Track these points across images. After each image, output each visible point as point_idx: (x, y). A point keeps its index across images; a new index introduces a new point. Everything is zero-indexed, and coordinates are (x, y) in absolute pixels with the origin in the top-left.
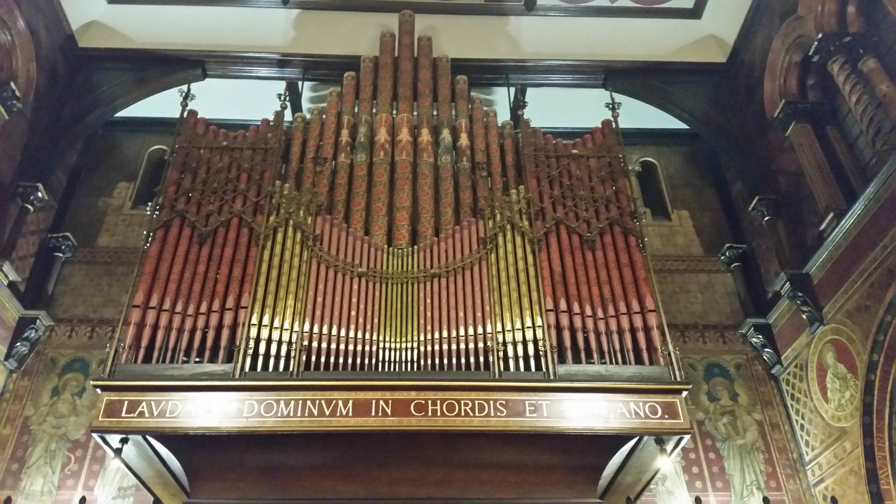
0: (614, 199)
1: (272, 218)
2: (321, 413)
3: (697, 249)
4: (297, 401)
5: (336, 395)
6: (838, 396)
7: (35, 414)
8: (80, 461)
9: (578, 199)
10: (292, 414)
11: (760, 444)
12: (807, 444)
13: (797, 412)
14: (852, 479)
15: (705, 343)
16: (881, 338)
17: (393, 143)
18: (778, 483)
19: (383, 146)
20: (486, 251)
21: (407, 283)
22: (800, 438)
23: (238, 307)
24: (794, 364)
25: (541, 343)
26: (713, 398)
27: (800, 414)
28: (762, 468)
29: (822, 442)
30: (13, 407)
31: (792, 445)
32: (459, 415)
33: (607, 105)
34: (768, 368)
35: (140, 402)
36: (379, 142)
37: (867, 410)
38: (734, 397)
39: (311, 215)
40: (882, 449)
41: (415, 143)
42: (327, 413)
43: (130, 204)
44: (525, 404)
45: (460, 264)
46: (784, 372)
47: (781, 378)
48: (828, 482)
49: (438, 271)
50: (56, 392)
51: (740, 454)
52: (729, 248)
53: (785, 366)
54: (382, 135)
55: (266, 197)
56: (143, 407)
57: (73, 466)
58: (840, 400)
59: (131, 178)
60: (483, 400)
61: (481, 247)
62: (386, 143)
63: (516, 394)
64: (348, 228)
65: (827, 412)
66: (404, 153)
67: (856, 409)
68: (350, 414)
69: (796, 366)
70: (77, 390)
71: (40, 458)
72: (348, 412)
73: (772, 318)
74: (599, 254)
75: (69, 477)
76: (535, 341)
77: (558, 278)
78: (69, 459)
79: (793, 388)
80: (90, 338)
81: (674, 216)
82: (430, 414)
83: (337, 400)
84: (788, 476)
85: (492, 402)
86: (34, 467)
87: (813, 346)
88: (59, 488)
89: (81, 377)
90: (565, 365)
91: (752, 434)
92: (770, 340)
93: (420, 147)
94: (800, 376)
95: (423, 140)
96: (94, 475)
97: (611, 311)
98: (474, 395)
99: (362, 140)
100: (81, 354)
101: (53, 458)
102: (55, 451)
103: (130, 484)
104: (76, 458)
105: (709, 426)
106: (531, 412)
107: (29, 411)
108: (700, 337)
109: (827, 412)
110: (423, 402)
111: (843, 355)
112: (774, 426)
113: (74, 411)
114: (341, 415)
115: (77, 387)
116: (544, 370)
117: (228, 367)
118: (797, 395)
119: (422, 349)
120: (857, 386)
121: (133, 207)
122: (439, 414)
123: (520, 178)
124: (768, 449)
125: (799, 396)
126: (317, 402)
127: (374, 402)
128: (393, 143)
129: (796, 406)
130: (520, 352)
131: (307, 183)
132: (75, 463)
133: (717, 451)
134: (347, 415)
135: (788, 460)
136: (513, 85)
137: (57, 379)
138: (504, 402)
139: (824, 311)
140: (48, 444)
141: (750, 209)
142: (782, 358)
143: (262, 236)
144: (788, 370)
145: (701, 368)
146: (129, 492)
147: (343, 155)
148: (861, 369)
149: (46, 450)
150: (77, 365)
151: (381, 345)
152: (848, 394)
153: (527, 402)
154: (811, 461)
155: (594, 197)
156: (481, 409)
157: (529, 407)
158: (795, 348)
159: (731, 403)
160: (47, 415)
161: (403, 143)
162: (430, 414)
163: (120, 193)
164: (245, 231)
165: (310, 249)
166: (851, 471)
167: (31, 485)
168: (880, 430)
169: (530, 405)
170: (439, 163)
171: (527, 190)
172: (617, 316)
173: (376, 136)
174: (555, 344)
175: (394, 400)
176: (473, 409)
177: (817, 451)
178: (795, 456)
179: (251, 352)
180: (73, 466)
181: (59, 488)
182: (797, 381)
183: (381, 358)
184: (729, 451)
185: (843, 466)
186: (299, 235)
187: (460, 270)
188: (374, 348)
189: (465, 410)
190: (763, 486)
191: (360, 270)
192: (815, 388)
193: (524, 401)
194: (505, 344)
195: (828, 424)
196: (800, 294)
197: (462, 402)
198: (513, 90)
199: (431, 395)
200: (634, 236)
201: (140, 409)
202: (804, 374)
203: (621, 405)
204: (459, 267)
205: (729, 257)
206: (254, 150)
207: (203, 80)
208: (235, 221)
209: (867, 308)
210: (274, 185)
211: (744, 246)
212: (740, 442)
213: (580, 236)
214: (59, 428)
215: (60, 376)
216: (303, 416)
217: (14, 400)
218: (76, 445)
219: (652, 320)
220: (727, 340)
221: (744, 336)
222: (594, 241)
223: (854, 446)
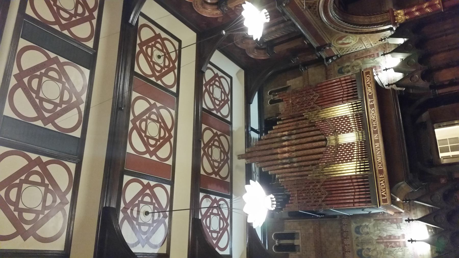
3: (301, 78)
6: (350, 40)
8: (391, 243)
9: (307, 99)
11: (362, 59)
12: (361, 48)
14: (372, 37)
15: (331, 74)
16: (340, 30)
17: (288, 152)
18: (372, 54)
19: (290, 154)
22: (359, 50)
24: (339, 51)
28: (368, 58)
29: (361, 44)
31: (361, 51)
32: (376, 119)
37: (356, 33)
38: (348, 66)
40: (366, 30)
41: (288, 146)
44: (371, 104)
46: (340, 54)
47: (341, 55)
48: (371, 42)
51: (365, 64)
52: (301, 69)
53: (338, 54)
54: (286, 155)
57: (393, 244)
58: (352, 40)
65: (354, 43)
66: (292, 148)
69: (339, 51)
70: (368, 251)
71: (391, 255)
75: (396, 245)
76: (352, 104)
78: (390, 247)
80: (349, 252)
81: (289, 85)
82: (376, 125)
84: (370, 52)
85: (371, 112)
87: (336, 46)
88: (400, 246)
89: (363, 251)
91: (359, 61)
92: (331, 57)
96: (395, 237)
100: (355, 253)
101: (391, 251)
102: (389, 251)
103: (396, 225)
104: (390, 244)
106: (372, 103)
112: (356, 56)
115: (367, 251)
116: (360, 101)
118: (347, 50)
119: (358, 131)
122: (376, 123)
125: (348, 50)
128: (288, 152)
129: (350, 51)
132: (391, 244)
135: (365, 52)
138: (371, 109)
139: (327, 43)
142: (336, 54)
146: (398, 225)
148: (347, 34)
150: (360, 253)
151: (358, 141)
152: (351, 38)
153: (370, 104)
162: (376, 125)
164: (326, 183)
166: (370, 37)
167: (400, 255)
168: (361, 30)
169: (371, 103)
173: (286, 157)
176: (374, 116)
177: (363, 45)
178: (364, 51)
180: (393, 244)
181: (400, 246)
182: (343, 50)
183: (362, 140)
184: (364, 67)
185: (368, 39)
186: (326, 168)
189: (374, 117)
190: (373, 58)
192: (347, 46)
197: (372, 118)
199: (371, 126)
205: (304, 69)
212: (361, 64)
214: (381, 252)
223: (363, 37)
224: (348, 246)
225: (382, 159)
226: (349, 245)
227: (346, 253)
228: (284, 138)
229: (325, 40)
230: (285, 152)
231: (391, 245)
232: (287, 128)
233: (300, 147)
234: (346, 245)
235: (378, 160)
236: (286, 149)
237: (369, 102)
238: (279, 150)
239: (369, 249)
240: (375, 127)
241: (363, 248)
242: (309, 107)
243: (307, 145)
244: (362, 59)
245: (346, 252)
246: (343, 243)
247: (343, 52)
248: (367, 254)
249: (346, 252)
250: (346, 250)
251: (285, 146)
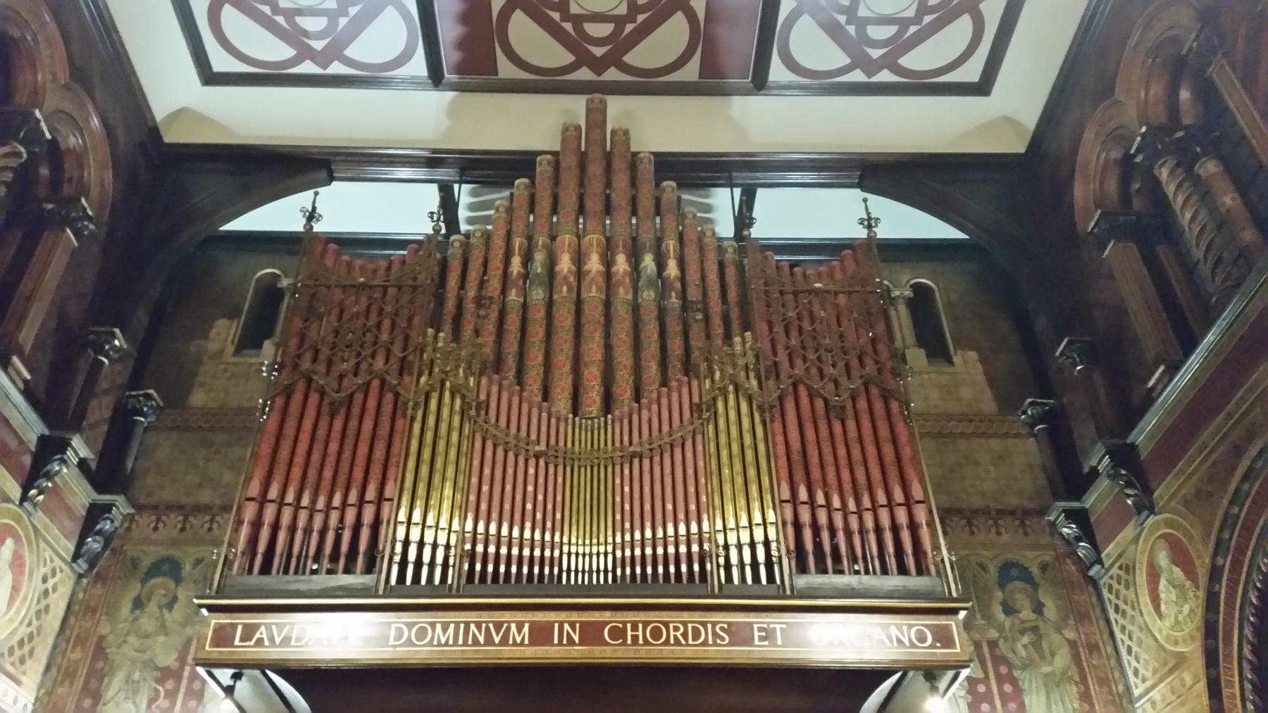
0: (870, 349)
1: (423, 379)
2: (489, 641)
3: (988, 405)
4: (457, 624)
5: (505, 616)
6: (1174, 609)
7: (111, 632)
8: (171, 696)
9: (822, 351)
10: (451, 642)
12: (1136, 673)
13: (1123, 629)
15: (999, 534)
16: (1226, 536)
17: (580, 273)
19: (565, 278)
20: (701, 421)
21: (599, 465)
22: (1127, 665)
23: (380, 498)
24: (1118, 564)
25: (774, 546)
26: (1009, 610)
27: (1127, 632)
29: (1155, 672)
30: (83, 623)
31: (1117, 674)
32: (667, 642)
33: (861, 222)
34: (1084, 567)
35: (257, 626)
36: (561, 274)
37: (1210, 630)
38: (1038, 609)
39: (474, 374)
40: (1230, 684)
41: (608, 274)
42: (497, 640)
43: (231, 349)
44: (752, 629)
45: (667, 440)
46: (1105, 574)
47: (1102, 582)
49: (638, 449)
50: (138, 604)
51: (1046, 686)
52: (1031, 404)
54: (565, 264)
55: (414, 351)
56: (261, 633)
58: (1176, 617)
59: (233, 314)
60: (701, 623)
61: (695, 415)
62: (569, 275)
63: (741, 614)
64: (522, 390)
65: (1160, 631)
67: (1198, 629)
68: (526, 642)
70: (166, 600)
71: (119, 691)
72: (523, 639)
73: (1090, 500)
74: (851, 425)
76: (767, 543)
77: (796, 457)
78: (157, 691)
79: (1118, 598)
80: (183, 529)
81: (957, 359)
82: (629, 642)
83: (509, 622)
85: (709, 626)
86: (111, 705)
87: (1141, 541)
90: (806, 576)
91: (1062, 660)
92: (1087, 531)
93: (614, 279)
94: (1126, 581)
95: (618, 270)
97: (866, 502)
98: (685, 616)
99: (539, 270)
100: (172, 552)
101: (136, 692)
102: (138, 682)
104: (166, 691)
105: (1003, 648)
106: (762, 639)
107: (104, 629)
108: (992, 526)
109: (1160, 631)
110: (621, 626)
111: (1181, 558)
112: (1093, 648)
113: (163, 629)
114: (515, 644)
115: (165, 596)
116: (778, 582)
117: (368, 580)
118: (1122, 606)
119: (619, 554)
120: (1197, 597)
121: (238, 351)
122: (641, 641)
123: (746, 326)
124: (1084, 681)
125: (1125, 607)
126: (484, 625)
127: (556, 625)
128: (580, 273)
129: (1121, 621)
130: (747, 559)
131: (467, 332)
132: (165, 697)
133: (1014, 682)
134: (522, 643)
135: (1111, 693)
136: (738, 185)
137: (139, 585)
138: (726, 626)
139: (1156, 494)
140: (131, 672)
141: (1057, 354)
142: (1103, 555)
143: (411, 404)
144: (1111, 572)
145: (993, 569)
147: (514, 292)
149: (128, 680)
150: (166, 567)
151: (566, 549)
152: (1186, 609)
153: (756, 626)
154: (1141, 697)
155: (843, 347)
156: (696, 635)
157: (759, 631)
158: (1118, 543)
159: (1033, 616)
160: (128, 634)
161: (592, 275)
162: (629, 642)
163: (219, 334)
164: (389, 397)
165: (472, 421)
168: (1228, 657)
169: (760, 630)
170: (640, 301)
171: (755, 339)
172: (874, 510)
174: (792, 547)
175: (583, 624)
176: (685, 635)
177: (1149, 683)
178: (1121, 688)
179: (397, 558)
182: (1121, 587)
183: (565, 567)
184: (1031, 681)
185: (1182, 704)
186: (458, 402)
187: (668, 447)
188: (557, 553)
189: (675, 637)
191: (537, 448)
192: (1145, 599)
193: (751, 624)
194: (726, 547)
195: (1164, 649)
196: (1123, 472)
197: (671, 626)
198: (737, 192)
199: (630, 616)
200: (896, 399)
201: (258, 635)
202: (1130, 578)
203: (879, 629)
204: (666, 443)
205: (1032, 417)
206: (399, 288)
207: (329, 184)
208: (376, 384)
209: (1210, 494)
210: (425, 334)
211: (1052, 401)
212: (1046, 669)
213: (826, 401)
215: (144, 581)
216: (465, 644)
217: (85, 615)
218: (166, 674)
219: (921, 514)
220: (1029, 530)
221: (1053, 525)
222: (843, 408)
223: (1193, 676)
224: (207, 526)
225: (442, 646)
226: (210, 530)
227: (181, 518)
228: (648, 262)
229: (1170, 477)
230: (579, 259)
231: (162, 693)
232: (699, 275)
233: (594, 313)
234: (212, 521)
235: (439, 627)
236: (594, 264)
237: (769, 623)
239: (171, 603)
240: (618, 633)
241: (183, 584)
243: (593, 349)
244: (1077, 678)
245: (186, 517)
247: (1116, 586)
248: (153, 597)
249: (186, 517)
250: (191, 519)
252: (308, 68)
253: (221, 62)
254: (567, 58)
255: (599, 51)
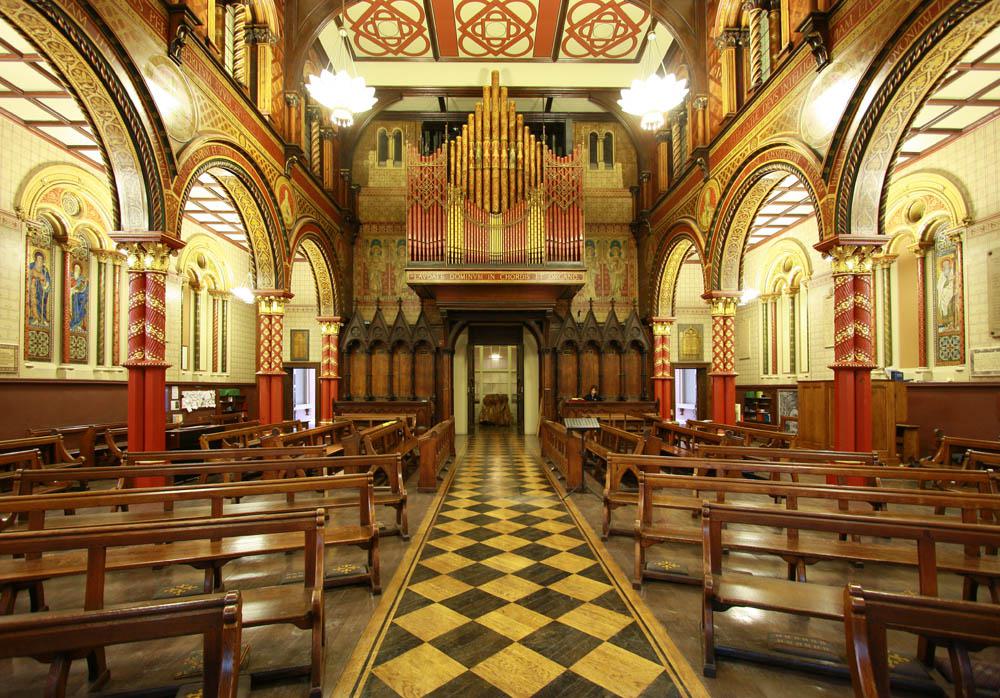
23: (442, 240)
26: (611, 255)
38: (620, 254)
43: (376, 164)
59: (375, 149)
105: (608, 267)
107: (365, 261)
128: (491, 158)
145: (609, 242)
230: (491, 153)
236: (496, 154)
238: (496, 143)
242: (550, 194)
246: (388, 223)
251: (500, 153)
252: (390, 55)
253: (359, 53)
254: (484, 51)
255: (496, 8)
